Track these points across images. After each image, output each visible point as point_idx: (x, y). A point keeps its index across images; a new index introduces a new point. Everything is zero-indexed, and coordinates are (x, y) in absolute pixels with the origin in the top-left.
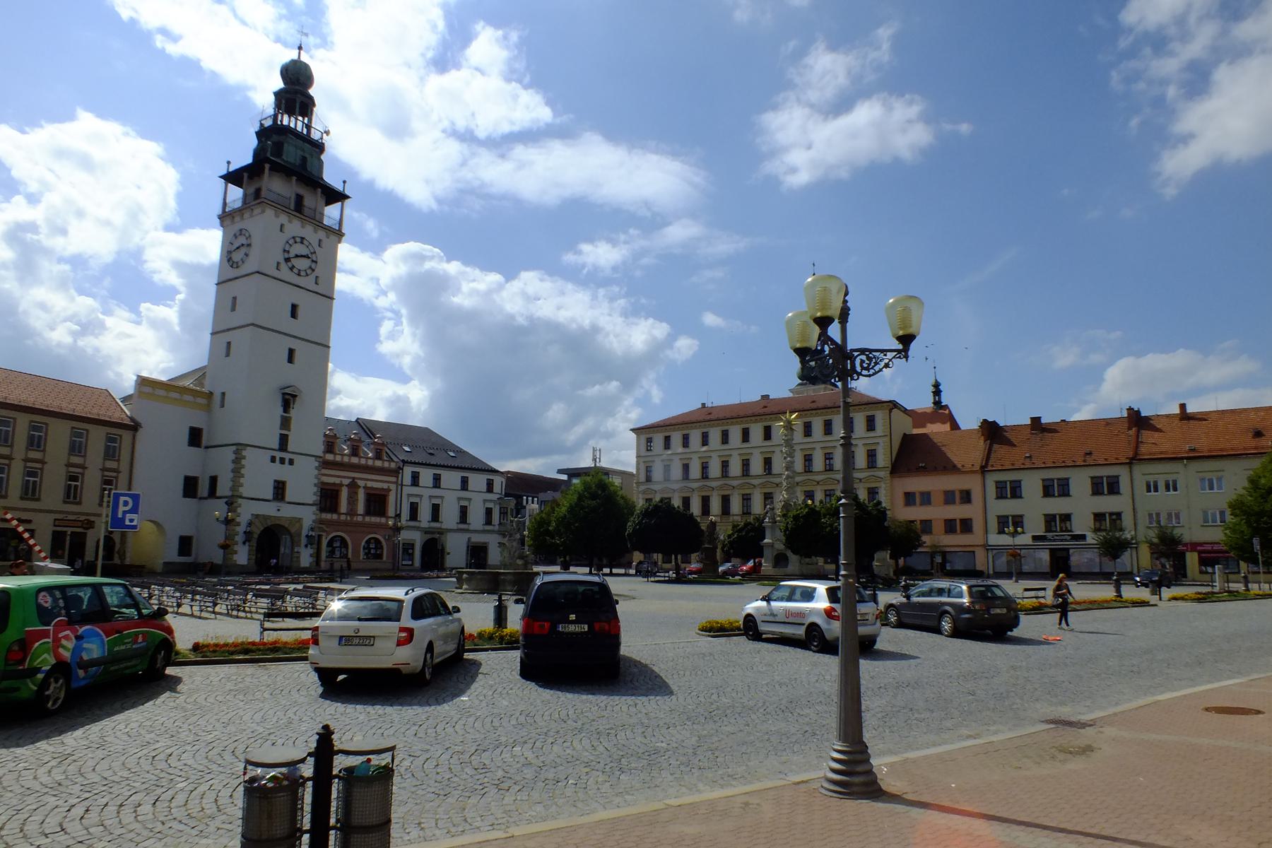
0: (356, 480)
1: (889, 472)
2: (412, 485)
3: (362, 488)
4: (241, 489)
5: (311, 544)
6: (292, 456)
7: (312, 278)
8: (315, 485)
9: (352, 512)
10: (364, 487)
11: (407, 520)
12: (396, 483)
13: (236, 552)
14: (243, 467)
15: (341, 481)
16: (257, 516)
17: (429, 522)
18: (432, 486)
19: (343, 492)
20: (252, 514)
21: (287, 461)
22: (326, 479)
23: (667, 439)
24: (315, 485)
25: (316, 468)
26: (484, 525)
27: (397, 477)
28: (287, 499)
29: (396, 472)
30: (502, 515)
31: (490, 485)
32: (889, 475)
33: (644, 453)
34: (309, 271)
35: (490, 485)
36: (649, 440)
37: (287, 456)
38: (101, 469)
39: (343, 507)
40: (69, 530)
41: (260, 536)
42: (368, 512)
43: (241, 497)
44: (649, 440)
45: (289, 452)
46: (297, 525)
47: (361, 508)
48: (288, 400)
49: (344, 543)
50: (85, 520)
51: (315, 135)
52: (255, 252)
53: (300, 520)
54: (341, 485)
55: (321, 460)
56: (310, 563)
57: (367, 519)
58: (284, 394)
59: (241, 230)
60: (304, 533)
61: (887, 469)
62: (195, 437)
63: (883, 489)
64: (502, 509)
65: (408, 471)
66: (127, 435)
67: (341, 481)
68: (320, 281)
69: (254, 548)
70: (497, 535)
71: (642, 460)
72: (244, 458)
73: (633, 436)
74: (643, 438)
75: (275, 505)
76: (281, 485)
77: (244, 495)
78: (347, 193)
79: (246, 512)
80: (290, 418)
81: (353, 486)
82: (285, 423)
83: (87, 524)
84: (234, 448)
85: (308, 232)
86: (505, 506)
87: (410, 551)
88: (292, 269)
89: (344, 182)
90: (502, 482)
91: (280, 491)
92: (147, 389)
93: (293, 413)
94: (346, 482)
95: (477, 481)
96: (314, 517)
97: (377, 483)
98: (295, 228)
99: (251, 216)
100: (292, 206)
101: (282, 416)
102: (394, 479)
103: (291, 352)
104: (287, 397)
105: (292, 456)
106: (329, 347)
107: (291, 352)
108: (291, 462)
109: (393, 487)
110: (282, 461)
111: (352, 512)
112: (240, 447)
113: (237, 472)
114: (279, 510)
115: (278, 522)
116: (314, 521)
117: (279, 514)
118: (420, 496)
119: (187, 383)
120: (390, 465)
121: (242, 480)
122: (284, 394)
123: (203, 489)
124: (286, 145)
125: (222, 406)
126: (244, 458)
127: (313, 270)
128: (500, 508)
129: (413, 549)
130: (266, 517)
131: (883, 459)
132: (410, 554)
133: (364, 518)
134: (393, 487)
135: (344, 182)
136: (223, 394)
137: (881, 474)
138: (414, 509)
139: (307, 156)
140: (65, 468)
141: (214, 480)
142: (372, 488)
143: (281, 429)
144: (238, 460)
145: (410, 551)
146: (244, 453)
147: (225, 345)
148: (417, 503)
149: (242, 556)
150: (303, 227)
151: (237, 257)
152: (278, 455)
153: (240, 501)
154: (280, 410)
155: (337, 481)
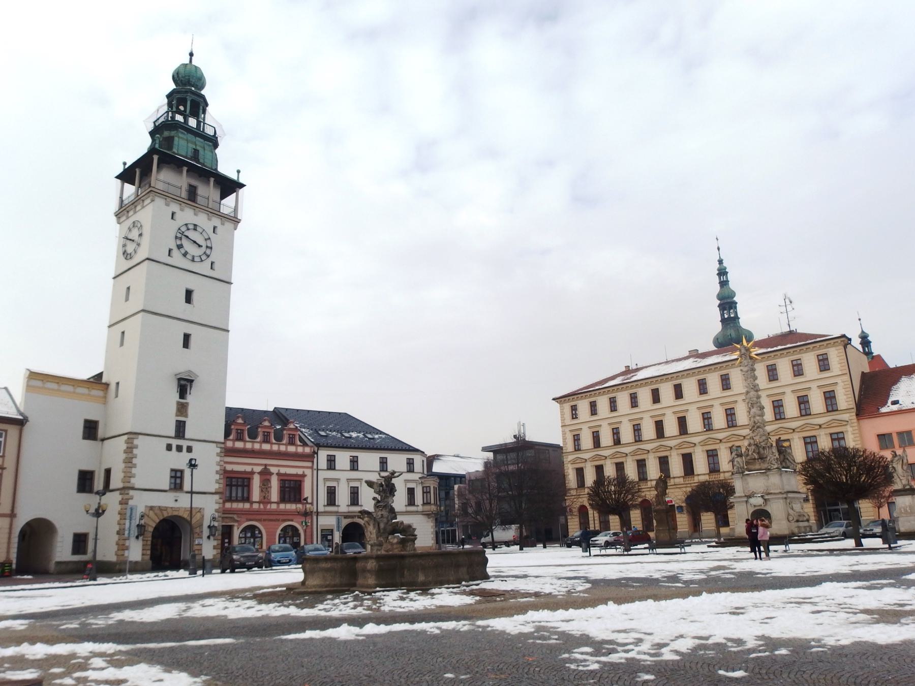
0: (268, 467)
1: (854, 414)
2: (351, 470)
3: (275, 474)
4: (133, 480)
5: (214, 535)
7: (207, 263)
8: (217, 472)
9: (265, 500)
10: (277, 474)
11: (324, 506)
12: (312, 468)
16: (152, 508)
17: (348, 506)
18: (326, 468)
19: (254, 480)
20: (146, 506)
21: (185, 449)
22: (229, 467)
23: (593, 406)
24: (217, 472)
25: (218, 455)
26: (406, 506)
27: (313, 462)
29: (311, 457)
30: (425, 494)
31: (410, 463)
32: (855, 417)
33: (569, 421)
34: (204, 257)
35: (410, 463)
36: (574, 408)
37: (184, 444)
39: (256, 495)
41: (155, 528)
42: (283, 499)
43: (133, 488)
44: (574, 408)
47: (274, 495)
48: (184, 385)
49: (295, 530)
51: (209, 131)
52: (145, 241)
54: (252, 473)
55: (223, 446)
56: (214, 555)
57: (282, 506)
58: (179, 379)
59: (134, 222)
60: (206, 523)
61: (853, 410)
62: (91, 430)
63: (850, 433)
64: (425, 489)
65: (323, 455)
66: (13, 431)
68: (216, 266)
69: (149, 543)
70: (421, 516)
71: (567, 429)
72: (136, 447)
73: (556, 405)
74: (567, 407)
75: (172, 495)
76: (179, 474)
77: (136, 486)
78: (241, 181)
79: (141, 502)
80: (187, 403)
81: (265, 474)
82: (182, 409)
84: (125, 437)
85: (202, 220)
86: (428, 485)
87: (330, 537)
88: (185, 254)
89: (238, 172)
90: (423, 461)
91: (178, 481)
92: (38, 383)
93: (190, 399)
94: (258, 469)
95: (397, 462)
96: (217, 506)
97: (292, 469)
98: (187, 215)
99: (143, 207)
100: (184, 194)
101: (178, 403)
102: (309, 464)
103: (187, 338)
104: (183, 382)
106: (228, 331)
107: (187, 338)
109: (308, 472)
110: (179, 449)
111: (265, 500)
112: (132, 436)
113: (129, 461)
114: (176, 500)
115: (175, 513)
116: (217, 511)
118: (337, 480)
119: (92, 380)
120: (304, 450)
121: (134, 471)
122: (179, 379)
123: (99, 484)
124: (176, 139)
125: (117, 396)
126: (136, 447)
127: (208, 256)
128: (423, 488)
129: (332, 535)
131: (845, 400)
132: (329, 541)
133: (278, 506)
134: (308, 472)
135: (238, 172)
136: (118, 384)
137: (846, 417)
138: (331, 494)
139: (198, 148)
141: (108, 472)
142: (285, 475)
143: (177, 415)
144: (130, 449)
145: (330, 537)
146: (136, 442)
147: (120, 335)
148: (335, 487)
149: (136, 552)
150: (195, 214)
151: (130, 248)
152: (175, 443)
153: (131, 492)
155: (248, 469)
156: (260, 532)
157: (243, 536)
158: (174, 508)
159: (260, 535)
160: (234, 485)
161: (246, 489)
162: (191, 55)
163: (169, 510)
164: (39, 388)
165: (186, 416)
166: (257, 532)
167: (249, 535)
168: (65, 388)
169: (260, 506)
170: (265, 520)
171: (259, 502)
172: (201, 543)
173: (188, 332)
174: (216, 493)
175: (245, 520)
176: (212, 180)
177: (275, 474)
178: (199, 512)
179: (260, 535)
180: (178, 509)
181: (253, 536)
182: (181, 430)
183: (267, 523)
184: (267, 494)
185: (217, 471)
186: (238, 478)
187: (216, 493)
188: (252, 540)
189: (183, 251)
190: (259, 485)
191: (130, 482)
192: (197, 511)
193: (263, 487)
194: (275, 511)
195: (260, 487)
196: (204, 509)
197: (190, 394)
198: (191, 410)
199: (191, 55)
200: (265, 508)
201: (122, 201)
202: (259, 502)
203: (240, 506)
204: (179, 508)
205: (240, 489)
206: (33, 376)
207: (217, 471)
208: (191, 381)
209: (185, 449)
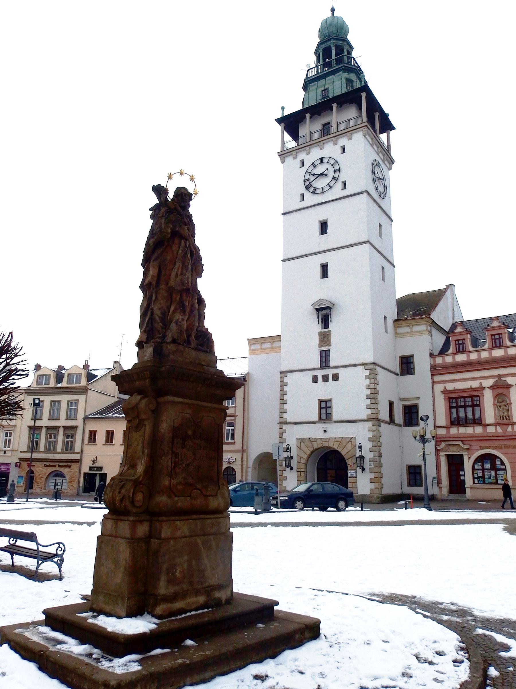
0: (502, 379)
4: (285, 415)
6: (335, 371)
13: (285, 479)
15: (481, 384)
20: (298, 439)
28: (335, 417)
37: (330, 373)
45: (333, 368)
46: (349, 446)
53: (351, 440)
54: (481, 389)
56: (371, 490)
67: (481, 384)
75: (320, 427)
76: (323, 405)
77: (288, 421)
88: (314, 192)
92: (257, 346)
94: (490, 382)
101: (320, 334)
105: (335, 371)
108: (336, 377)
110: (325, 379)
114: (325, 431)
121: (285, 406)
122: (318, 310)
130: (311, 440)
143: (320, 346)
146: (285, 380)
152: (320, 374)
154: (317, 328)
155: (475, 384)
156: (503, 463)
157: (480, 467)
159: (503, 467)
160: (461, 407)
161: (477, 409)
162: (333, 10)
163: (319, 441)
164: (270, 348)
165: (330, 345)
166: (498, 463)
167: (487, 466)
169: (496, 429)
170: (506, 447)
171: (495, 425)
172: (355, 475)
173: (324, 261)
174: (368, 420)
175: (478, 447)
176: (334, 105)
177: (486, 389)
179: (503, 467)
180: (327, 440)
181: (494, 467)
182: (324, 358)
183: (510, 450)
184: (506, 414)
185: (367, 396)
186: (464, 397)
187: (368, 420)
188: (493, 473)
189: (311, 190)
190: (492, 402)
191: (283, 417)
192: (348, 440)
193: (498, 404)
194: (480, 435)
195: (494, 405)
196: (355, 438)
197: (385, 318)
198: (334, 338)
199: (333, 10)
200: (505, 431)
201: (323, 173)
202: (495, 425)
203: (469, 430)
204: (329, 439)
205: (469, 410)
206: (252, 341)
207: (367, 396)
208: (329, 308)
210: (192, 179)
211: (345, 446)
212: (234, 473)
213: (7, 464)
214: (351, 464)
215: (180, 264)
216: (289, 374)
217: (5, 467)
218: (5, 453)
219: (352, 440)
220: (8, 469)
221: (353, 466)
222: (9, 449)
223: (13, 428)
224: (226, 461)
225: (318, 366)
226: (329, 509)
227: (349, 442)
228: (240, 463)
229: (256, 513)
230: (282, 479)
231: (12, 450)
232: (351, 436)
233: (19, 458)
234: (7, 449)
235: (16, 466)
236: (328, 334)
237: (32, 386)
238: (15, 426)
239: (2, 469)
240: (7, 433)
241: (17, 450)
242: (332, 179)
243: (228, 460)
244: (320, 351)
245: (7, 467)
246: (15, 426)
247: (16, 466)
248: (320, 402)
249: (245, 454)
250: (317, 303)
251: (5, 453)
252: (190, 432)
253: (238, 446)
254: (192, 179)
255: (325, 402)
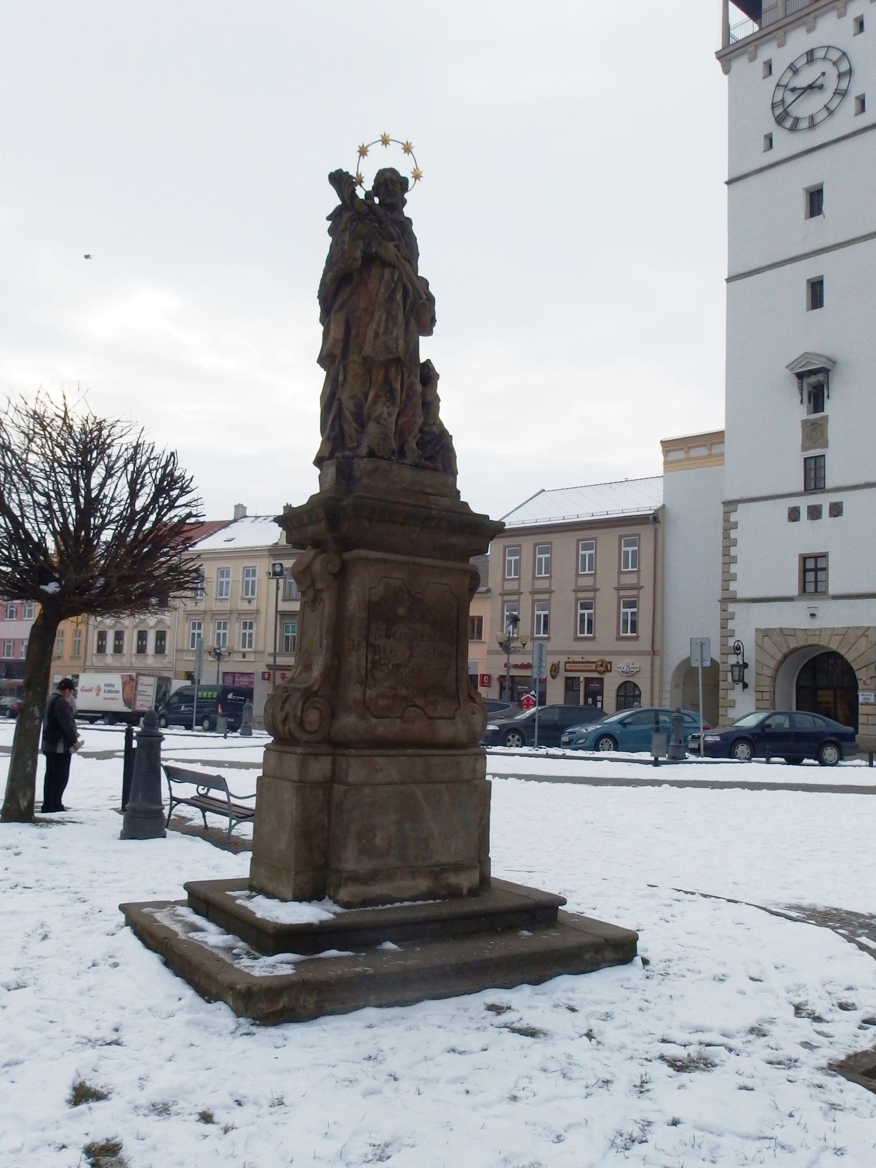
4: (733, 586)
6: (835, 498)
13: (733, 705)
14: (734, 543)
20: (757, 630)
28: (834, 588)
37: (824, 501)
38: (500, 594)
40: (582, 676)
50: (599, 661)
66: (646, 533)
77: (739, 596)
80: (825, 419)
83: (601, 665)
88: (793, 129)
92: (680, 455)
93: (830, 406)
101: (805, 424)
105: (835, 498)
108: (836, 510)
110: (815, 513)
114: (813, 615)
117: (817, 624)
121: (733, 569)
122: (800, 376)
140: (573, 594)
143: (804, 448)
146: (733, 518)
152: (803, 503)
154: (800, 412)
158: (810, 630)
164: (705, 457)
165: (825, 445)
168: (696, 452)
173: (813, 274)
178: (863, 635)
180: (817, 633)
189: (788, 123)
192: (860, 633)
198: (833, 431)
201: (813, 83)
204: (821, 630)
206: (668, 446)
208: (825, 371)
209: (826, 511)
210: (407, 149)
211: (853, 644)
212: (637, 693)
213: (249, 675)
214: (864, 679)
215: (382, 315)
216: (740, 506)
217: (247, 680)
218: (244, 656)
219: (869, 632)
220: (252, 683)
221: (868, 682)
222: (250, 650)
223: (255, 615)
224: (623, 672)
225: (800, 487)
226: (805, 761)
227: (860, 637)
228: (648, 675)
229: (656, 763)
230: (725, 705)
231: (255, 652)
232: (868, 625)
233: (267, 665)
234: (247, 649)
235: (263, 678)
236: (821, 424)
237: (280, 544)
238: (258, 611)
239: (242, 683)
240: (245, 624)
241: (263, 652)
242: (835, 93)
243: (625, 668)
244: (806, 460)
245: (250, 680)
246: (258, 611)
247: (263, 678)
248: (804, 559)
249: (657, 659)
250: (799, 361)
251: (244, 656)
252: (401, 611)
253: (644, 643)
254: (407, 149)
255: (814, 559)
